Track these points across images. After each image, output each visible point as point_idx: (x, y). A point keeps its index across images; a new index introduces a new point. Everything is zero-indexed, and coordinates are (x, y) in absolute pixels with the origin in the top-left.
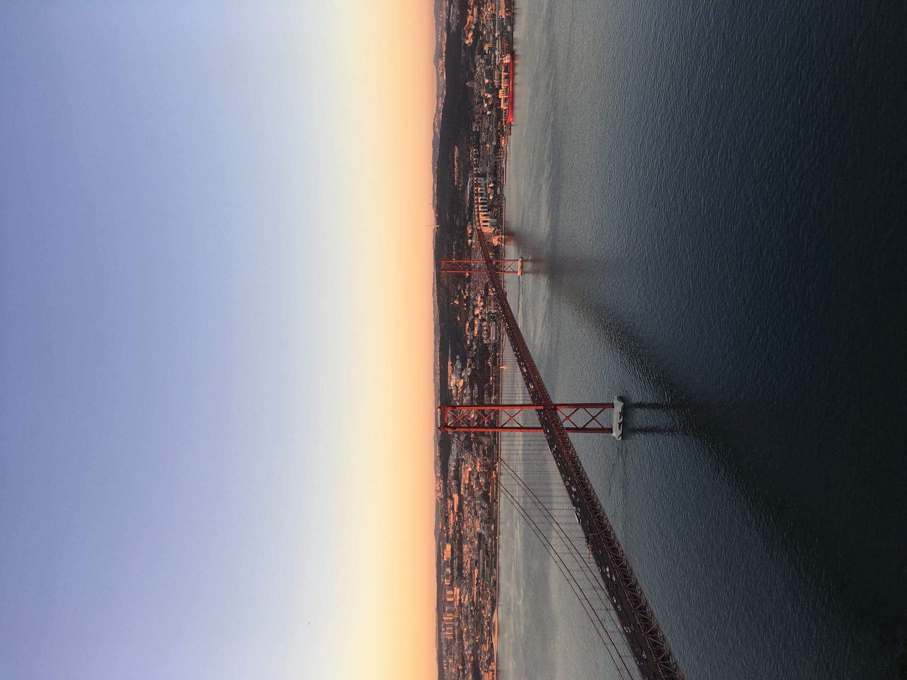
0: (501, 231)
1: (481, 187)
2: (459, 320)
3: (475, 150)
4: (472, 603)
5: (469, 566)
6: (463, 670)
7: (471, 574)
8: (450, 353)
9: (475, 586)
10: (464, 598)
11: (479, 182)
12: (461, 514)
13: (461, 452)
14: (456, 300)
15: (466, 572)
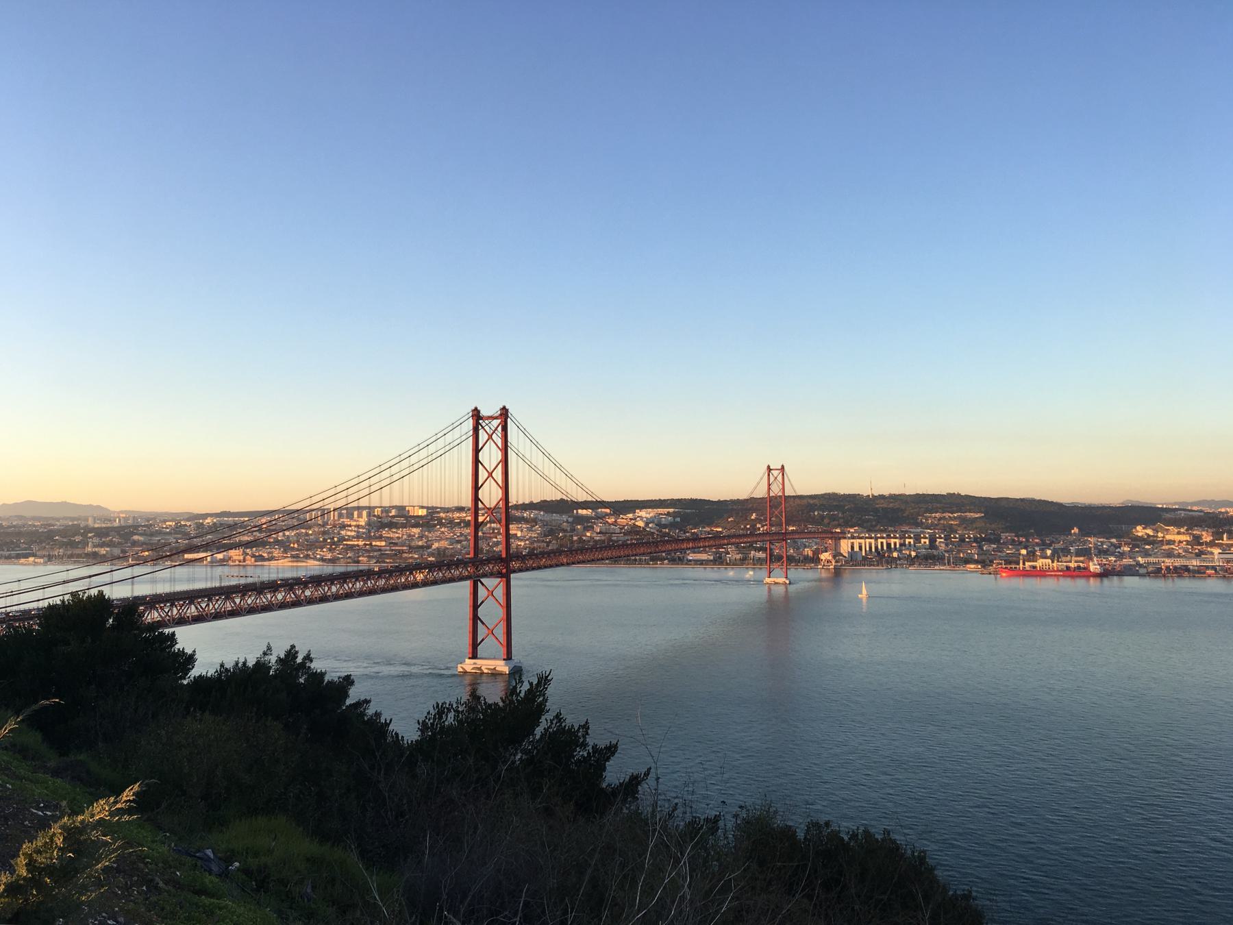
0: (841, 566)
1: (915, 543)
2: (729, 520)
3: (972, 536)
4: (342, 539)
5: (392, 535)
6: (260, 531)
7: (380, 538)
8: (686, 511)
9: (363, 543)
10: (351, 531)
11: (923, 540)
12: (462, 525)
13: (545, 524)
14: (757, 515)
15: (385, 533)
